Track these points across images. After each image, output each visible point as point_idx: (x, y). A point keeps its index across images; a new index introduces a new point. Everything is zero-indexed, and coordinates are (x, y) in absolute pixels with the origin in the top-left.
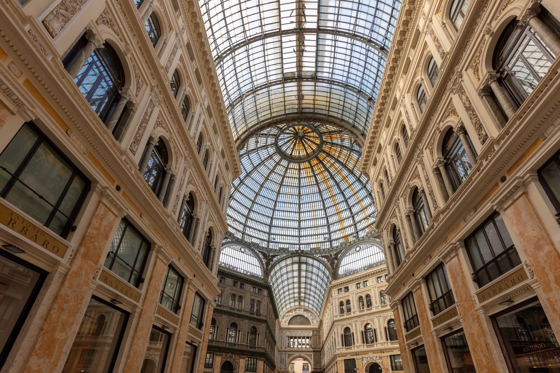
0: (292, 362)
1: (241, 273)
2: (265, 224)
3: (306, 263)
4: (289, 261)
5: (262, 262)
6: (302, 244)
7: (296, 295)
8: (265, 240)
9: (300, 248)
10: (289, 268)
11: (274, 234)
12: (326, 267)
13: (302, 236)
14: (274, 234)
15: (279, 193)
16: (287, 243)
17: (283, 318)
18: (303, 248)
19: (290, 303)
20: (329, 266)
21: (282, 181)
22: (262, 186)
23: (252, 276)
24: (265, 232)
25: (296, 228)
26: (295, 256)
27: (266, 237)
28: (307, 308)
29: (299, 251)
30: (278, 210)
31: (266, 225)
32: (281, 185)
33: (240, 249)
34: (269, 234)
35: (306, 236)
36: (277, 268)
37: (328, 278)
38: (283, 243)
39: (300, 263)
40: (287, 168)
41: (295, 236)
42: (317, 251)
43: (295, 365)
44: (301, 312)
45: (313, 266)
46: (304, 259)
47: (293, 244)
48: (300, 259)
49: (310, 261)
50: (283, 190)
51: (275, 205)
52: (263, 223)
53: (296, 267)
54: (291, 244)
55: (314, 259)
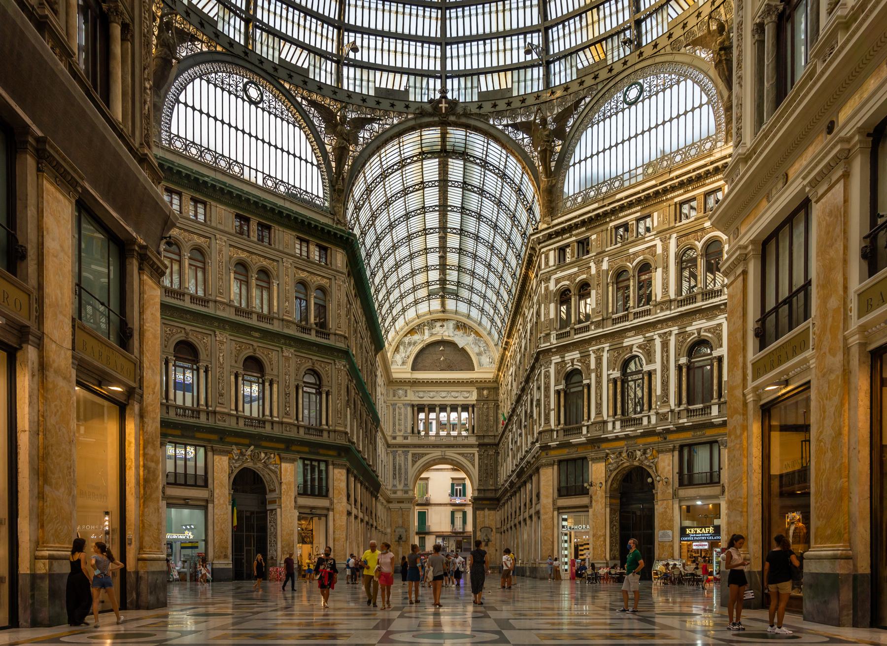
0: (422, 476)
1: (255, 186)
3: (464, 155)
5: (321, 145)
20: (537, 163)
23: (293, 196)
26: (429, 125)
33: (245, 90)
36: (372, 169)
39: (444, 153)
43: (430, 483)
45: (485, 164)
49: (477, 144)
53: (431, 167)
55: (490, 135)
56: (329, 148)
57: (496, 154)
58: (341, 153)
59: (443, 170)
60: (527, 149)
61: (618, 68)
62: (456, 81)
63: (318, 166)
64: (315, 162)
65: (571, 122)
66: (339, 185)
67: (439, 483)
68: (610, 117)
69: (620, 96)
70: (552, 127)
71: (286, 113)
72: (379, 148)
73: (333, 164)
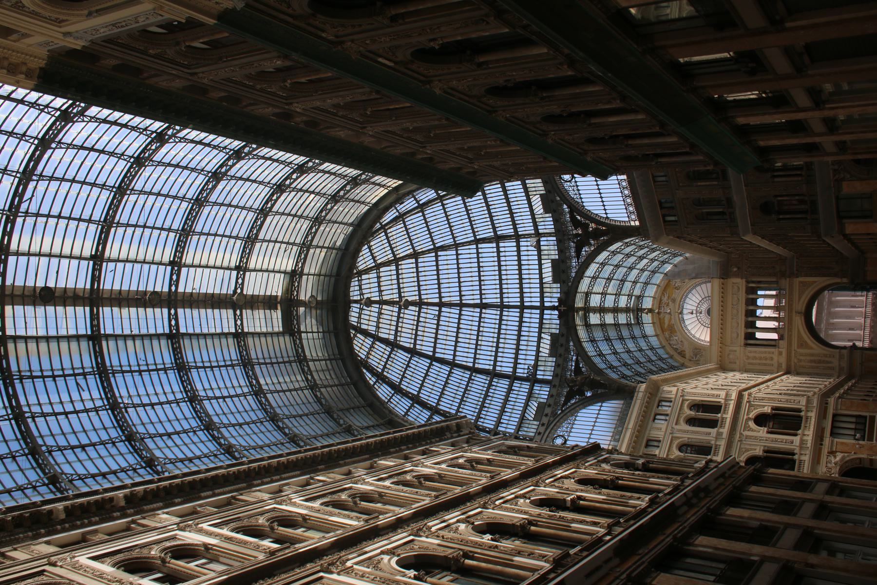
2: (488, 388)
4: (582, 333)
6: (542, 301)
8: (531, 389)
9: (553, 308)
11: (515, 368)
13: (522, 301)
14: (515, 368)
15: (413, 352)
16: (540, 338)
18: (552, 300)
24: (510, 390)
25: (501, 315)
29: (562, 308)
30: (454, 355)
31: (490, 385)
35: (522, 293)
39: (587, 310)
41: (521, 317)
47: (541, 323)
50: (406, 341)
51: (442, 361)
53: (594, 319)
58: (593, 385)
59: (595, 310)
62: (546, 299)
68: (578, 190)
72: (588, 356)
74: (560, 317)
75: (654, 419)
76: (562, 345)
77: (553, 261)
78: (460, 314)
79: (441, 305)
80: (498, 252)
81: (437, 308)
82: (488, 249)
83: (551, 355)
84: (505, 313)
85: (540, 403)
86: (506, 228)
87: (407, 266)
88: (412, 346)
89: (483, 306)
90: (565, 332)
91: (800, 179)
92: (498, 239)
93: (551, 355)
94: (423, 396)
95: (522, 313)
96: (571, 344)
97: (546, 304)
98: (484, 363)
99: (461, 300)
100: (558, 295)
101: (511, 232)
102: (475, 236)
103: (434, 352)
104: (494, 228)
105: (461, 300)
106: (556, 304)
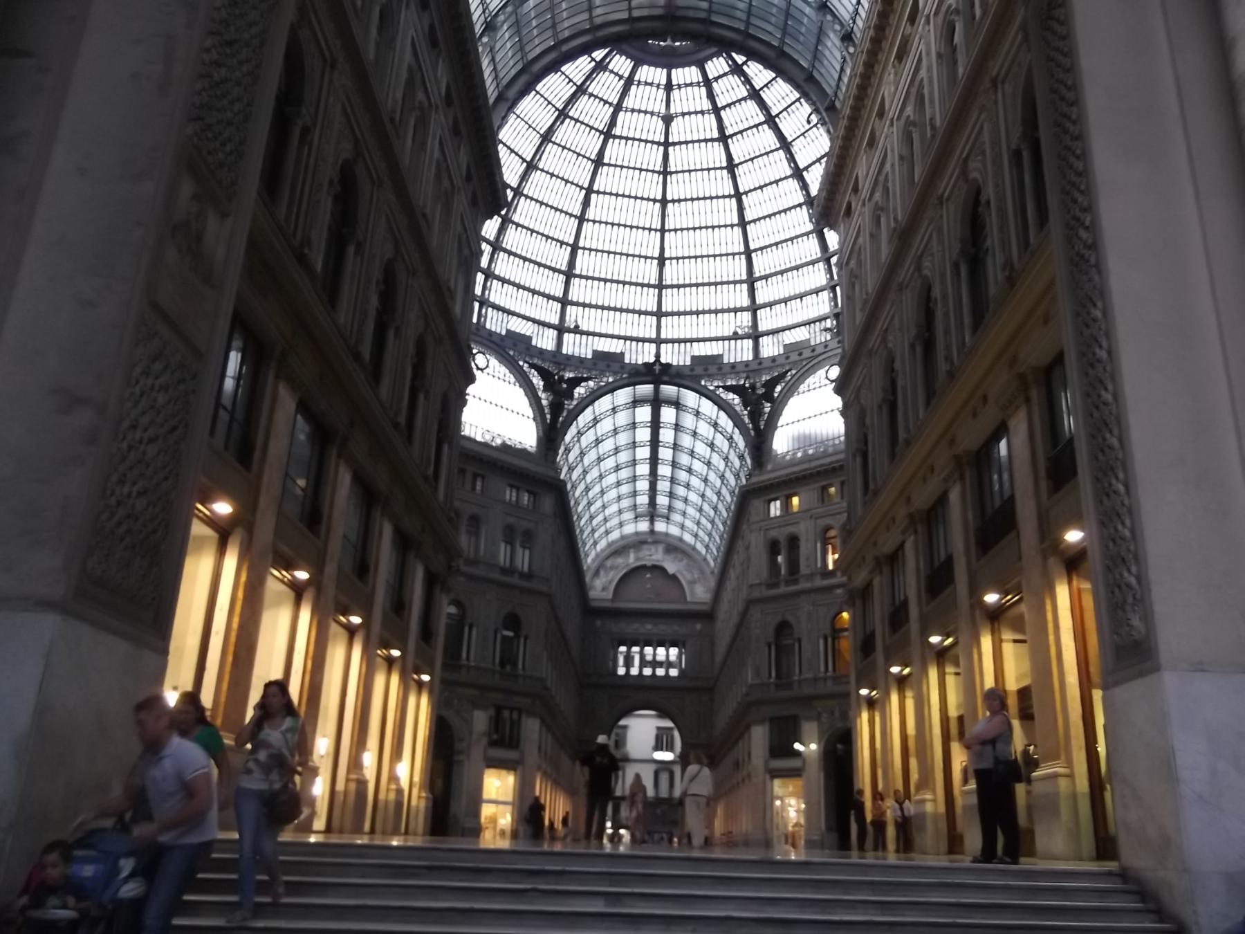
3: (677, 404)
4: (623, 396)
6: (667, 341)
7: (643, 500)
8: (549, 326)
9: (658, 355)
10: (622, 418)
11: (577, 304)
12: (737, 421)
13: (667, 314)
14: (577, 304)
15: (598, 162)
17: (597, 573)
18: (670, 355)
19: (621, 525)
20: (747, 420)
21: (613, 122)
22: (547, 137)
24: (549, 297)
25: (649, 286)
27: (550, 313)
28: (677, 543)
29: (657, 368)
31: (554, 270)
32: (608, 135)
34: (564, 302)
35: (679, 314)
36: (585, 417)
37: (741, 457)
38: (606, 336)
39: (656, 403)
40: (629, 82)
41: (646, 313)
42: (713, 369)
44: (656, 556)
46: (668, 390)
47: (638, 340)
48: (657, 390)
49: (690, 398)
50: (615, 151)
51: (586, 203)
52: (545, 266)
53: (644, 413)
54: (632, 339)
55: (704, 393)
56: (544, 402)
57: (707, 407)
58: (556, 407)
60: (738, 408)
61: (820, 350)
63: (534, 419)
64: (532, 416)
65: (778, 389)
66: (551, 434)
67: (641, 732)
69: (821, 373)
70: (761, 391)
71: (508, 374)
72: (592, 402)
73: (548, 416)
74: (646, 365)
75: (512, 486)
76: (608, 366)
77: (720, 356)
78: (650, 230)
79: (664, 202)
80: (735, 282)
81: (659, 197)
82: (738, 268)
83: (595, 352)
84: (651, 290)
85: (530, 338)
86: (764, 293)
87: (716, 154)
88: (606, 160)
89: (662, 260)
90: (627, 369)
91: (822, 669)
92: (751, 281)
93: (595, 352)
94: (536, 176)
95: (651, 314)
96: (611, 380)
97: (663, 346)
98: (584, 263)
99: (670, 231)
100: (675, 363)
101: (760, 299)
102: (756, 250)
103: (598, 192)
104: (766, 277)
105: (670, 231)
106: (663, 360)
